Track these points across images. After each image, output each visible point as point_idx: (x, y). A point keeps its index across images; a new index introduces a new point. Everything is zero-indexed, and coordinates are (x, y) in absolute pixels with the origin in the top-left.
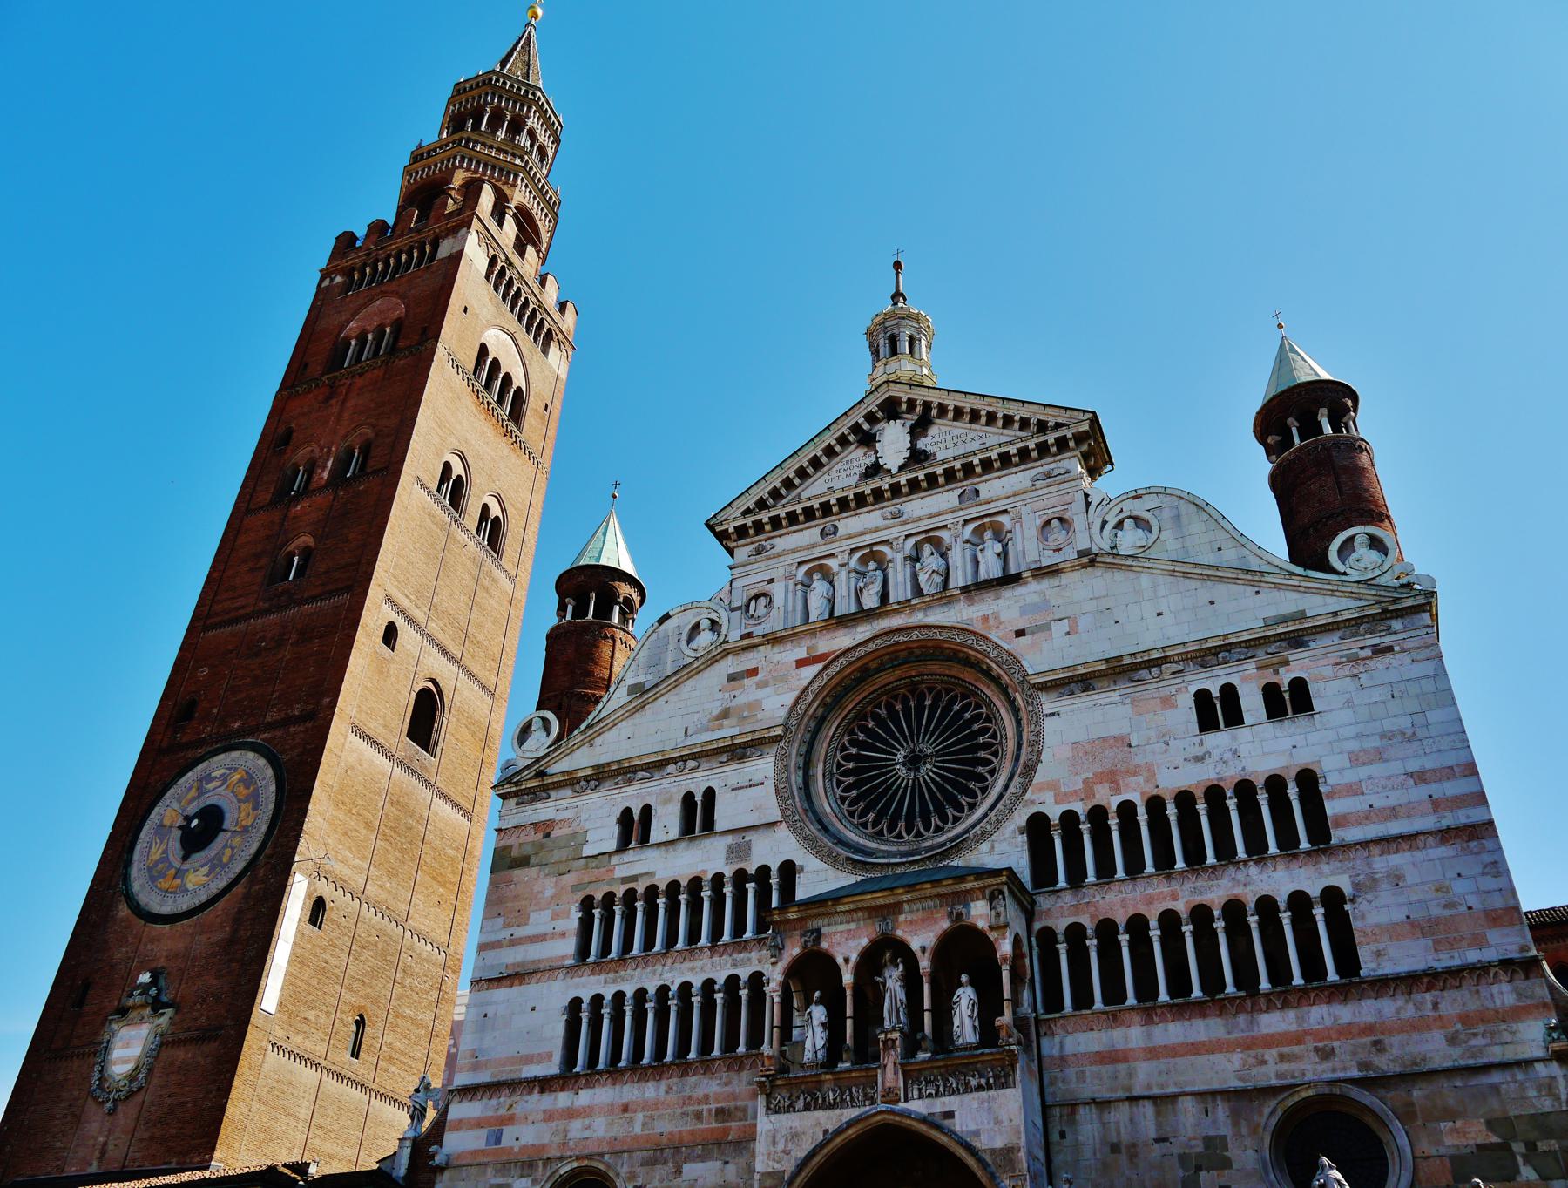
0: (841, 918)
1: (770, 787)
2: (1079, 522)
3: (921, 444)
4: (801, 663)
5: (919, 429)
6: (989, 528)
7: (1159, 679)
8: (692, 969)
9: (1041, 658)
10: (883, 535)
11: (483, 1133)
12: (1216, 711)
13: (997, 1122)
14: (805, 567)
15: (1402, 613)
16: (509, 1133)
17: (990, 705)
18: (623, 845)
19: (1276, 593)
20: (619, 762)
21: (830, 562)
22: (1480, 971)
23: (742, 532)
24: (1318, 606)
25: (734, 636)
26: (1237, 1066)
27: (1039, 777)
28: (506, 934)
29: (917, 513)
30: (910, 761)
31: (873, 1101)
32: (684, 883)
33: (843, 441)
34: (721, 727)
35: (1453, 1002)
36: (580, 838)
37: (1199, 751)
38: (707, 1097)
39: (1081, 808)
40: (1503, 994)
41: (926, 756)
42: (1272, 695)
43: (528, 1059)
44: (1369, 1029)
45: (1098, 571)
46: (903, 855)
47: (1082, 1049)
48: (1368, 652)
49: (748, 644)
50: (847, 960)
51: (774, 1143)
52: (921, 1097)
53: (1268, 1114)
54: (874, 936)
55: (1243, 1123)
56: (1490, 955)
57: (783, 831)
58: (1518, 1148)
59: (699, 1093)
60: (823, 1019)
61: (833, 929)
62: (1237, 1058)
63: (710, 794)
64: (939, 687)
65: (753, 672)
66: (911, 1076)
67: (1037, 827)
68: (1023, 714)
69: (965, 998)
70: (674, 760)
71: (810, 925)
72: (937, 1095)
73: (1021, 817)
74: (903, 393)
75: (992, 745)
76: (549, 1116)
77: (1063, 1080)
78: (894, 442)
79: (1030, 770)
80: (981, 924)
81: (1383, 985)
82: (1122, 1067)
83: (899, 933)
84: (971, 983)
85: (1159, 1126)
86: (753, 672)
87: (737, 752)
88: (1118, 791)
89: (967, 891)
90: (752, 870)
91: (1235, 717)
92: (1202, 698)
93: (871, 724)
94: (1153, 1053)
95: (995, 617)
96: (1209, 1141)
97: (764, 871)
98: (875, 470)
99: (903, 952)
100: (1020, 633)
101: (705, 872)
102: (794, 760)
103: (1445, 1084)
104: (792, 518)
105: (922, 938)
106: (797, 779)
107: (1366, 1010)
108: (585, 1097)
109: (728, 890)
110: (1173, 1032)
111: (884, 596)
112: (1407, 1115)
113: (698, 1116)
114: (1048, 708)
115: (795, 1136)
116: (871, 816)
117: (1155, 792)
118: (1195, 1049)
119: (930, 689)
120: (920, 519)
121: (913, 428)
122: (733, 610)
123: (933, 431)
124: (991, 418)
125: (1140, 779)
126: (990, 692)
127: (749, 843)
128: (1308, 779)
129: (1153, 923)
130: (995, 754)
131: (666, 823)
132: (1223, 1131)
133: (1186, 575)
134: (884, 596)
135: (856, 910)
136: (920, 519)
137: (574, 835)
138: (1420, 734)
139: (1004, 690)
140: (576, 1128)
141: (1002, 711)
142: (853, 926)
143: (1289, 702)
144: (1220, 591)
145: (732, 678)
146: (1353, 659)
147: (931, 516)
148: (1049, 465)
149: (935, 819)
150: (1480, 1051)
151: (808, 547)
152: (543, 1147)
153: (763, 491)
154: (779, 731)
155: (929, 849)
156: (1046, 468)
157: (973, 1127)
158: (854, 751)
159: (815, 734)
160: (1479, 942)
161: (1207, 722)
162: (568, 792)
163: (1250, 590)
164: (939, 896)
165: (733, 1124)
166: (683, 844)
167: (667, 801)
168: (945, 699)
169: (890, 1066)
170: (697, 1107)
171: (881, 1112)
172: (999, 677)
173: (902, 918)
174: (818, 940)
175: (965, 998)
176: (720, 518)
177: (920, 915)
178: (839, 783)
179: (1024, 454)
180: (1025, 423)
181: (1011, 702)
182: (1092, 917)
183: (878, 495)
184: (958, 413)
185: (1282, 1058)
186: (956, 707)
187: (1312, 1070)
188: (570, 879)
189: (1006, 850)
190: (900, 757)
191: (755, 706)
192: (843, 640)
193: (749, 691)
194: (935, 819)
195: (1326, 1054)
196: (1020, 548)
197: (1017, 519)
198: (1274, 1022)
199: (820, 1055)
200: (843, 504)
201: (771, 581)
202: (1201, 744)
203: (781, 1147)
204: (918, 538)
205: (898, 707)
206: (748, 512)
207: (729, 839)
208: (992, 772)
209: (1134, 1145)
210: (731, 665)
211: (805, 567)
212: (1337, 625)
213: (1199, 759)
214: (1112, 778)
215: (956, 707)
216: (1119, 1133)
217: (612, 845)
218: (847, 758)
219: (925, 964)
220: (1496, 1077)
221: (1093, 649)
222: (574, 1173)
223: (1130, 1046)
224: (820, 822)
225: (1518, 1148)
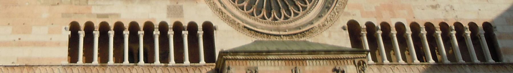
28: (16, 37)
32: (141, 25)
39: (377, 23)
46: (275, 30)
67: (353, 28)
73: (344, 22)
88: (394, 16)
90: (185, 24)
97: (192, 28)
109: (171, 33)
117: (413, 20)
127: (181, 7)
149: (283, 12)
155: (290, 30)
194: (283, 12)
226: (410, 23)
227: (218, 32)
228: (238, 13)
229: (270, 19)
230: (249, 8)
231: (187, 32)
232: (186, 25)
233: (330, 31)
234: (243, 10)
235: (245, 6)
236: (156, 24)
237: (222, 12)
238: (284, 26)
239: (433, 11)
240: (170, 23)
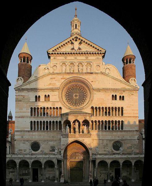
1: (57, 96)
2: (101, 66)
3: (80, 47)
4: (61, 79)
5: (80, 43)
6: (89, 63)
9: (95, 85)
10: (74, 61)
11: (21, 136)
12: (114, 97)
14: (62, 63)
15: (135, 90)
16: (24, 137)
18: (36, 100)
19: (123, 84)
20: (35, 88)
21: (66, 63)
22: (134, 131)
23: (52, 54)
24: (127, 87)
25: (51, 72)
29: (79, 59)
33: (68, 42)
34: (50, 86)
35: (131, 133)
36: (29, 99)
40: (135, 133)
42: (120, 97)
43: (26, 128)
44: (123, 135)
45: (103, 75)
48: (131, 94)
49: (53, 74)
53: (112, 142)
56: (135, 130)
57: (60, 103)
58: (133, 147)
59: (50, 134)
62: (110, 136)
63: (49, 96)
65: (54, 78)
67: (92, 108)
74: (79, 37)
76: (30, 135)
78: (76, 44)
79: (92, 101)
80: (88, 120)
81: (125, 131)
86: (54, 78)
87: (52, 90)
91: (116, 99)
92: (113, 96)
94: (102, 135)
95: (89, 78)
98: (73, 49)
99: (78, 121)
100: (92, 82)
102: (61, 93)
103: (128, 140)
104: (60, 54)
105: (81, 121)
106: (61, 96)
107: (123, 133)
108: (34, 133)
110: (104, 133)
111: (73, 71)
112: (125, 143)
113: (50, 137)
116: (70, 102)
118: (106, 135)
120: (79, 60)
121: (79, 43)
122: (51, 67)
123: (82, 45)
124: (91, 46)
126: (87, 88)
128: (122, 108)
130: (86, 97)
131: (42, 98)
133: (113, 79)
134: (73, 71)
136: (79, 60)
137: (28, 98)
138: (134, 105)
140: (34, 137)
143: (122, 98)
144: (117, 82)
145: (51, 78)
146: (129, 95)
147: (81, 60)
148: (98, 56)
150: (132, 138)
151: (63, 60)
152: (29, 139)
153: (56, 48)
154: (59, 88)
156: (97, 57)
159: (63, 89)
160: (134, 128)
161: (113, 99)
162: (25, 91)
163: (120, 83)
166: (45, 102)
167: (42, 95)
176: (49, 51)
178: (66, 97)
179: (95, 53)
180: (96, 48)
183: (74, 53)
184: (86, 43)
185: (115, 137)
187: (117, 139)
188: (29, 104)
189: (89, 111)
190: (74, 95)
191: (55, 84)
192: (68, 76)
193: (54, 81)
195: (119, 137)
196: (93, 68)
197: (93, 64)
198: (115, 133)
200: (68, 53)
201: (57, 64)
204: (79, 63)
206: (53, 51)
207: (52, 103)
210: (51, 76)
211: (62, 63)
212: (129, 90)
217: (35, 101)
220: (133, 141)
221: (101, 87)
222: (33, 142)
225: (133, 147)
228: (68, 105)
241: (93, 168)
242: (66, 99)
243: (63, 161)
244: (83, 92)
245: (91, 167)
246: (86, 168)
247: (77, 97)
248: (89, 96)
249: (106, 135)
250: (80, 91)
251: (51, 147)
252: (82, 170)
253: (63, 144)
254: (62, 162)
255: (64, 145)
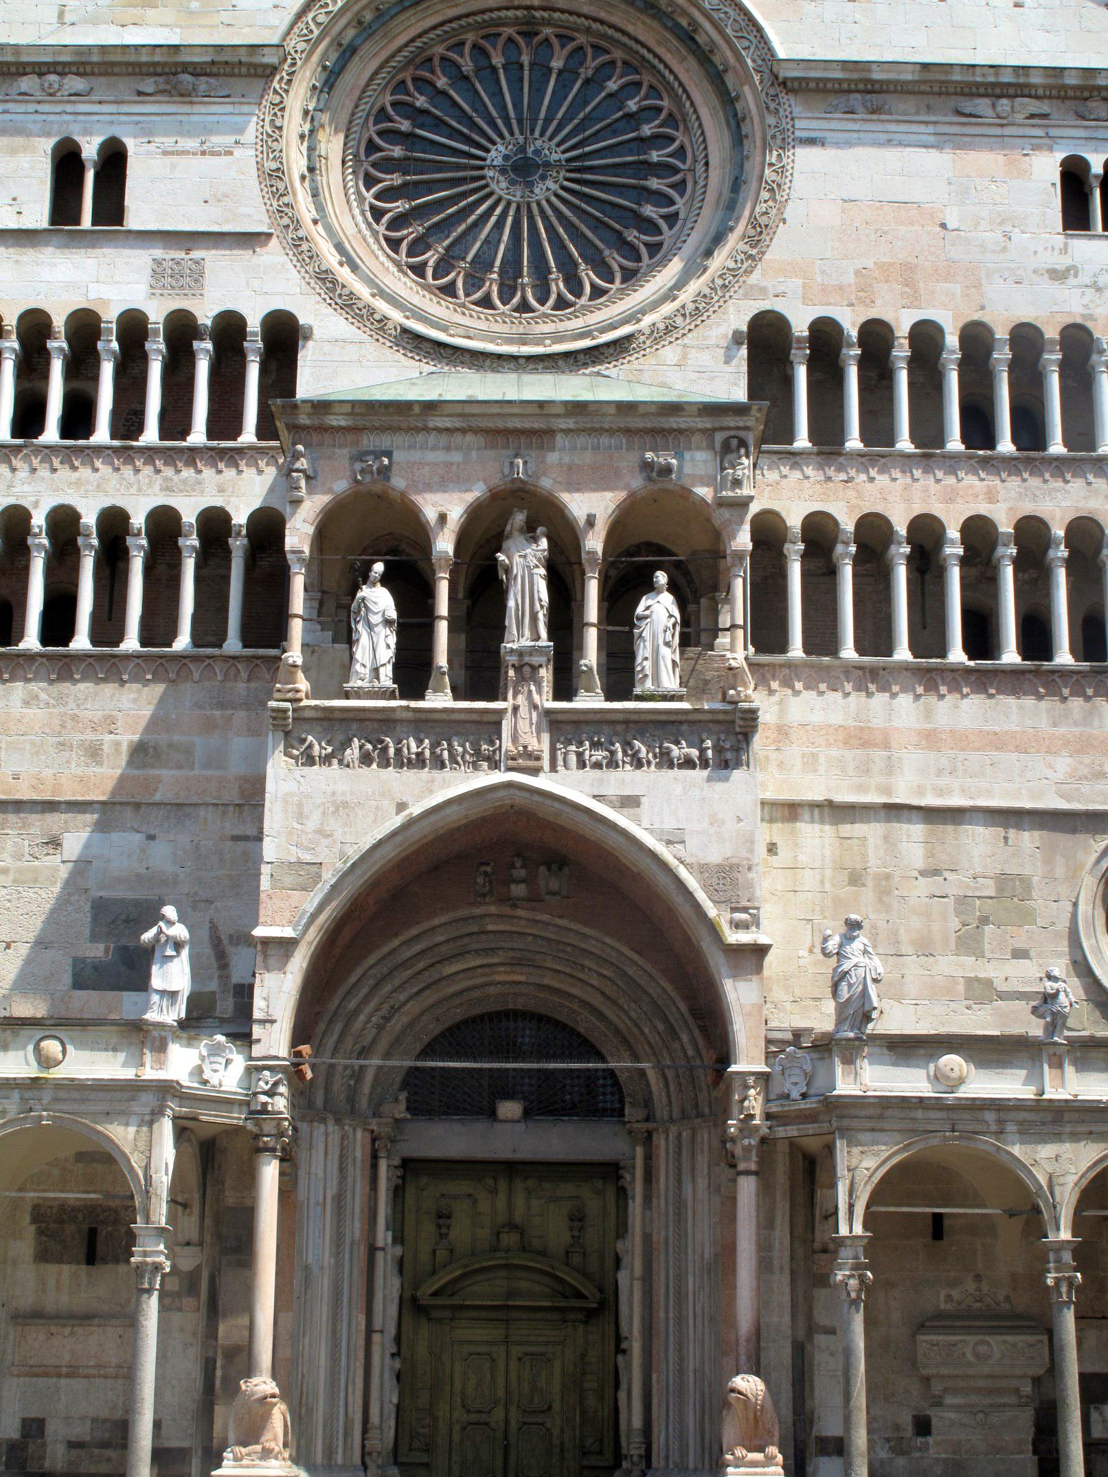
0: (432, 438)
7: (1003, 121)
8: (78, 484)
13: (714, 821)
17: (679, 94)
26: (1060, 776)
27: (779, 249)
30: (516, 168)
31: (495, 765)
37: (1061, 262)
38: (109, 724)
41: (547, 164)
46: (509, 341)
47: (817, 718)
50: (443, 518)
51: (300, 816)
52: (582, 764)
54: (496, 481)
55: (1059, 860)
60: (393, 614)
61: (416, 456)
64: (581, 39)
66: (563, 728)
68: (754, 127)
69: (659, 610)
70: (41, 70)
71: (369, 441)
72: (613, 764)
73: (738, 315)
75: (676, 171)
77: (781, 765)
82: (879, 755)
83: (546, 483)
84: (673, 588)
85: (930, 854)
88: (914, 303)
89: (681, 431)
90: (205, 315)
93: (442, 82)
94: (930, 739)
96: (1003, 880)
97: (229, 330)
101: (105, 303)
109: (156, 348)
110: (966, 711)
114: (804, 126)
115: (341, 807)
116: (431, 257)
117: (976, 316)
118: (997, 742)
119: (564, 39)
125: (957, 288)
126: (687, 72)
129: (953, 533)
130: (680, 187)
132: (1026, 872)
135: (464, 431)
139: (717, 78)
141: (704, 113)
142: (457, 457)
155: (558, 338)
157: (669, 824)
158: (405, 126)
164: (628, 431)
165: (166, 774)
168: (591, 64)
169: (523, 711)
170: (89, 736)
171: (510, 785)
172: (713, 47)
173: (553, 457)
174: (385, 472)
175: (659, 610)
177: (587, 457)
181: (728, 100)
182: (851, 508)
186: (612, 86)
189: (710, 372)
190: (496, 154)
194: (558, 285)
199: (387, 673)
202: (1064, 250)
203: (312, 823)
205: (498, 60)
208: (672, 219)
209: (888, 877)
213: (1058, 275)
214: (907, 276)
215: (612, 86)
216: (864, 856)
218: (391, 135)
219: (595, 543)
223: (897, 723)
224: (339, 247)
226: (960, 325)
227: (310, 344)
229: (546, 309)
230: (443, 267)
231: (208, 345)
232: (209, 323)
233: (685, 346)
234: (422, 275)
235: (431, 263)
236: (110, 315)
237: (334, 282)
238: (548, 328)
239: (1054, 288)
240: (156, 314)
241: (782, 1284)
242: (377, 214)
243: (285, 1158)
244: (632, 119)
245: (764, 1265)
246: (681, 1277)
247: (545, 189)
248: (717, 177)
249: (997, 742)
250: (580, 101)
251: (100, 908)
252: (603, 1308)
253: (294, 854)
254: (270, 1173)
255: (307, 872)
